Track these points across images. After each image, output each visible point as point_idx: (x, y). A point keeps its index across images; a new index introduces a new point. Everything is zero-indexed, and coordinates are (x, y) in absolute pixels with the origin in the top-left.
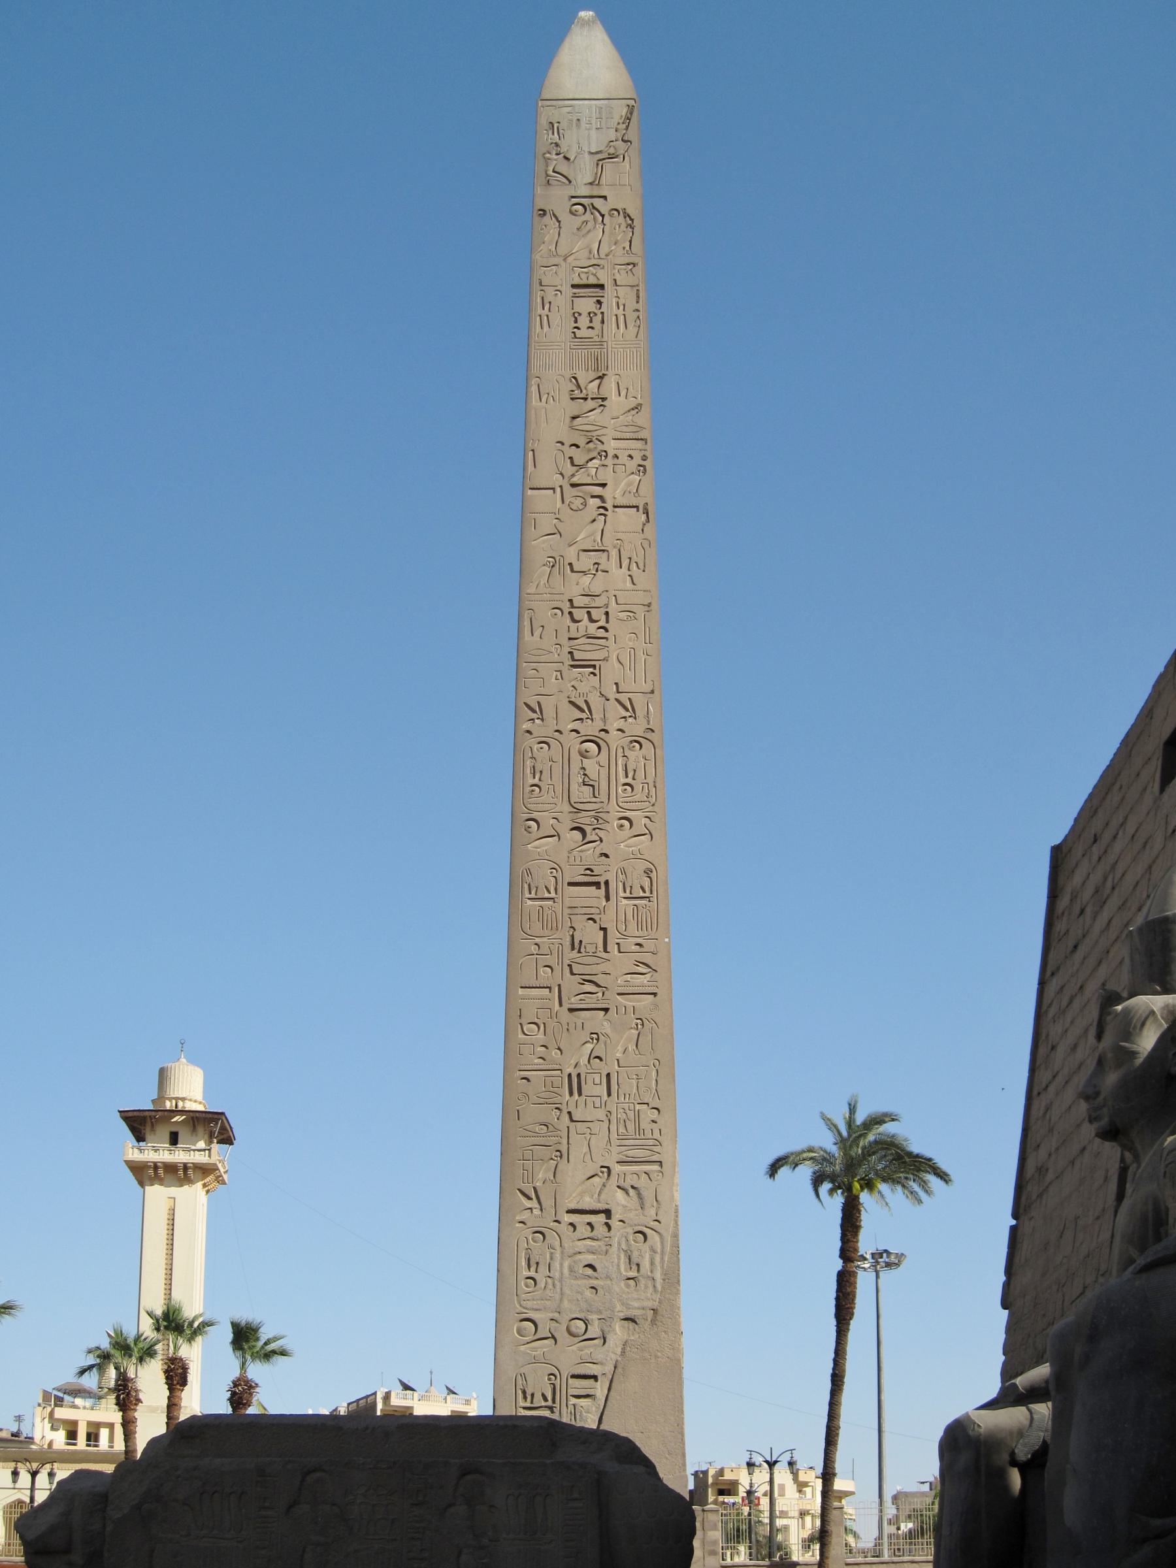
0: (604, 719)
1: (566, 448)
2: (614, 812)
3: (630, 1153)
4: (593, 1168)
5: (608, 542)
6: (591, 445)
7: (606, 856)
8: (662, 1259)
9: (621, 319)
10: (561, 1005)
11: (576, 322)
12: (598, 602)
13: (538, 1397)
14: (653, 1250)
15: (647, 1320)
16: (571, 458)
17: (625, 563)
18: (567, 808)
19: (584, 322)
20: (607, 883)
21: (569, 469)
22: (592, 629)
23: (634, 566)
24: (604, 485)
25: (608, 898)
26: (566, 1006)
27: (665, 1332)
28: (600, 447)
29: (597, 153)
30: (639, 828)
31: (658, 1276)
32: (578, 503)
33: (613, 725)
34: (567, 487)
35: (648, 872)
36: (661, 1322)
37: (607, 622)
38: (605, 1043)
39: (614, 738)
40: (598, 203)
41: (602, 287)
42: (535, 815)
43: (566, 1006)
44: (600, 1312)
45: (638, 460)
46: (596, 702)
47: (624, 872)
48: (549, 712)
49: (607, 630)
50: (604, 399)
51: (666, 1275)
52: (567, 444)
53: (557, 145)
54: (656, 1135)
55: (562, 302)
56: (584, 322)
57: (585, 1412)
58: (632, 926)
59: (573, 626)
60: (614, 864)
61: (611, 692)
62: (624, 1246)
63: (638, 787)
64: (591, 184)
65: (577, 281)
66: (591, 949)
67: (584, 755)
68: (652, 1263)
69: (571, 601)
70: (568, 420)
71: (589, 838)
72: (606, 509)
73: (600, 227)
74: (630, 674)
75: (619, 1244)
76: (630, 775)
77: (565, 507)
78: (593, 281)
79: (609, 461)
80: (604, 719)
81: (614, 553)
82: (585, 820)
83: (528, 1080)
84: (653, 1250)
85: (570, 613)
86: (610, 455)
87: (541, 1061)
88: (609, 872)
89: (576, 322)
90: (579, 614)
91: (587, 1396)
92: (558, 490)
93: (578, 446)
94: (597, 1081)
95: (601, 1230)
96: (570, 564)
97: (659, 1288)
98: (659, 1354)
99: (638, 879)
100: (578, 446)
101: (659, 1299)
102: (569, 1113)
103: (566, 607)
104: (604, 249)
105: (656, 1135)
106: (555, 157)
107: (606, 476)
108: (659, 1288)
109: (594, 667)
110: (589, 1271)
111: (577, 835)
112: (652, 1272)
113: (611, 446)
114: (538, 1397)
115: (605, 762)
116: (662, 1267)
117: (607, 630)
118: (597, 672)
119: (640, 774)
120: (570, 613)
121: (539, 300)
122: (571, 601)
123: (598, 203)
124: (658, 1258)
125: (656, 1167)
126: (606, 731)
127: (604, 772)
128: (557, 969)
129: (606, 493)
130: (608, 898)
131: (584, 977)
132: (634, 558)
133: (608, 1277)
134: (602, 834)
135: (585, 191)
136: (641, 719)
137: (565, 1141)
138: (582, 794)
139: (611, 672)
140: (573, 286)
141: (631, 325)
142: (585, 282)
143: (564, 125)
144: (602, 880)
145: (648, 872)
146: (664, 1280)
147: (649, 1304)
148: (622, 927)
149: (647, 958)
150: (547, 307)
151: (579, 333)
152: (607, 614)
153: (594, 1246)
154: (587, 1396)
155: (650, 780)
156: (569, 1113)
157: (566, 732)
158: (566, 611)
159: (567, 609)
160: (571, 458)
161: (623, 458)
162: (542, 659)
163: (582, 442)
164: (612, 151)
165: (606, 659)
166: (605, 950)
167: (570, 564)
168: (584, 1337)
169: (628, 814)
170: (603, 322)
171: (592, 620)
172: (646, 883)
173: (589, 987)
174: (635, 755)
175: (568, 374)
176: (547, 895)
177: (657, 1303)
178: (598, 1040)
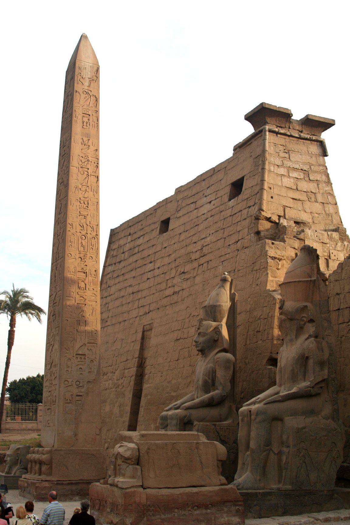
0: (87, 230)
1: (80, 157)
2: (89, 255)
3: (90, 341)
4: (82, 344)
5: (89, 184)
6: (86, 158)
7: (87, 266)
9: (94, 125)
10: (75, 302)
11: (83, 123)
12: (87, 199)
13: (69, 400)
16: (81, 160)
17: (92, 190)
18: (78, 252)
19: (85, 124)
20: (86, 272)
21: (80, 163)
22: (85, 206)
23: (94, 191)
24: (88, 169)
25: (86, 276)
26: (76, 302)
28: (88, 159)
29: (89, 78)
30: (94, 259)
32: (82, 173)
33: (89, 232)
34: (80, 168)
35: (96, 271)
37: (88, 205)
38: (85, 313)
39: (89, 235)
40: (89, 92)
41: (89, 115)
42: (71, 253)
43: (76, 302)
45: (96, 164)
46: (85, 226)
47: (90, 270)
48: (74, 227)
49: (88, 207)
50: (89, 146)
52: (80, 156)
53: (80, 73)
54: (96, 337)
55: (80, 117)
56: (85, 124)
58: (92, 284)
59: (80, 204)
60: (88, 268)
61: (88, 223)
63: (94, 249)
64: (88, 86)
65: (84, 112)
66: (82, 289)
67: (82, 238)
69: (80, 198)
70: (81, 150)
71: (83, 260)
72: (89, 175)
73: (89, 99)
74: (93, 220)
76: (92, 246)
77: (79, 173)
78: (87, 113)
79: (90, 163)
80: (87, 230)
81: (90, 187)
82: (82, 255)
83: (68, 320)
85: (80, 201)
86: (90, 161)
87: (70, 316)
88: (87, 270)
89: (83, 123)
90: (82, 202)
91: (80, 400)
92: (78, 168)
93: (83, 157)
94: (83, 322)
95: (83, 360)
96: (80, 188)
99: (93, 273)
100: (83, 157)
102: (77, 330)
103: (79, 199)
104: (90, 105)
105: (96, 337)
106: (80, 76)
107: (89, 166)
109: (85, 216)
110: (81, 370)
111: (80, 259)
113: (90, 159)
114: (69, 400)
115: (86, 242)
117: (88, 207)
118: (85, 218)
119: (94, 246)
120: (80, 201)
121: (75, 115)
122: (80, 198)
123: (89, 92)
125: (96, 345)
126: (87, 234)
127: (86, 245)
128: (75, 293)
129: (89, 171)
130: (86, 276)
132: (95, 190)
134: (86, 260)
135: (86, 88)
136: (95, 232)
137: (75, 336)
138: (81, 249)
139: (89, 218)
140: (83, 113)
141: (96, 128)
142: (85, 113)
143: (82, 68)
144: (85, 272)
145: (96, 271)
148: (89, 284)
149: (95, 293)
150: (76, 118)
151: (84, 127)
152: (88, 203)
154: (80, 400)
155: (97, 247)
156: (77, 330)
157: (78, 232)
158: (79, 200)
159: (79, 200)
160: (81, 160)
161: (93, 162)
162: (73, 212)
163: (84, 156)
164: (93, 79)
165: (88, 215)
166: (86, 290)
167: (80, 188)
168: (79, 386)
169: (92, 256)
170: (89, 125)
171: (84, 204)
172: (95, 273)
173: (82, 298)
174: (93, 240)
175: (81, 137)
176: (73, 274)
178: (84, 312)
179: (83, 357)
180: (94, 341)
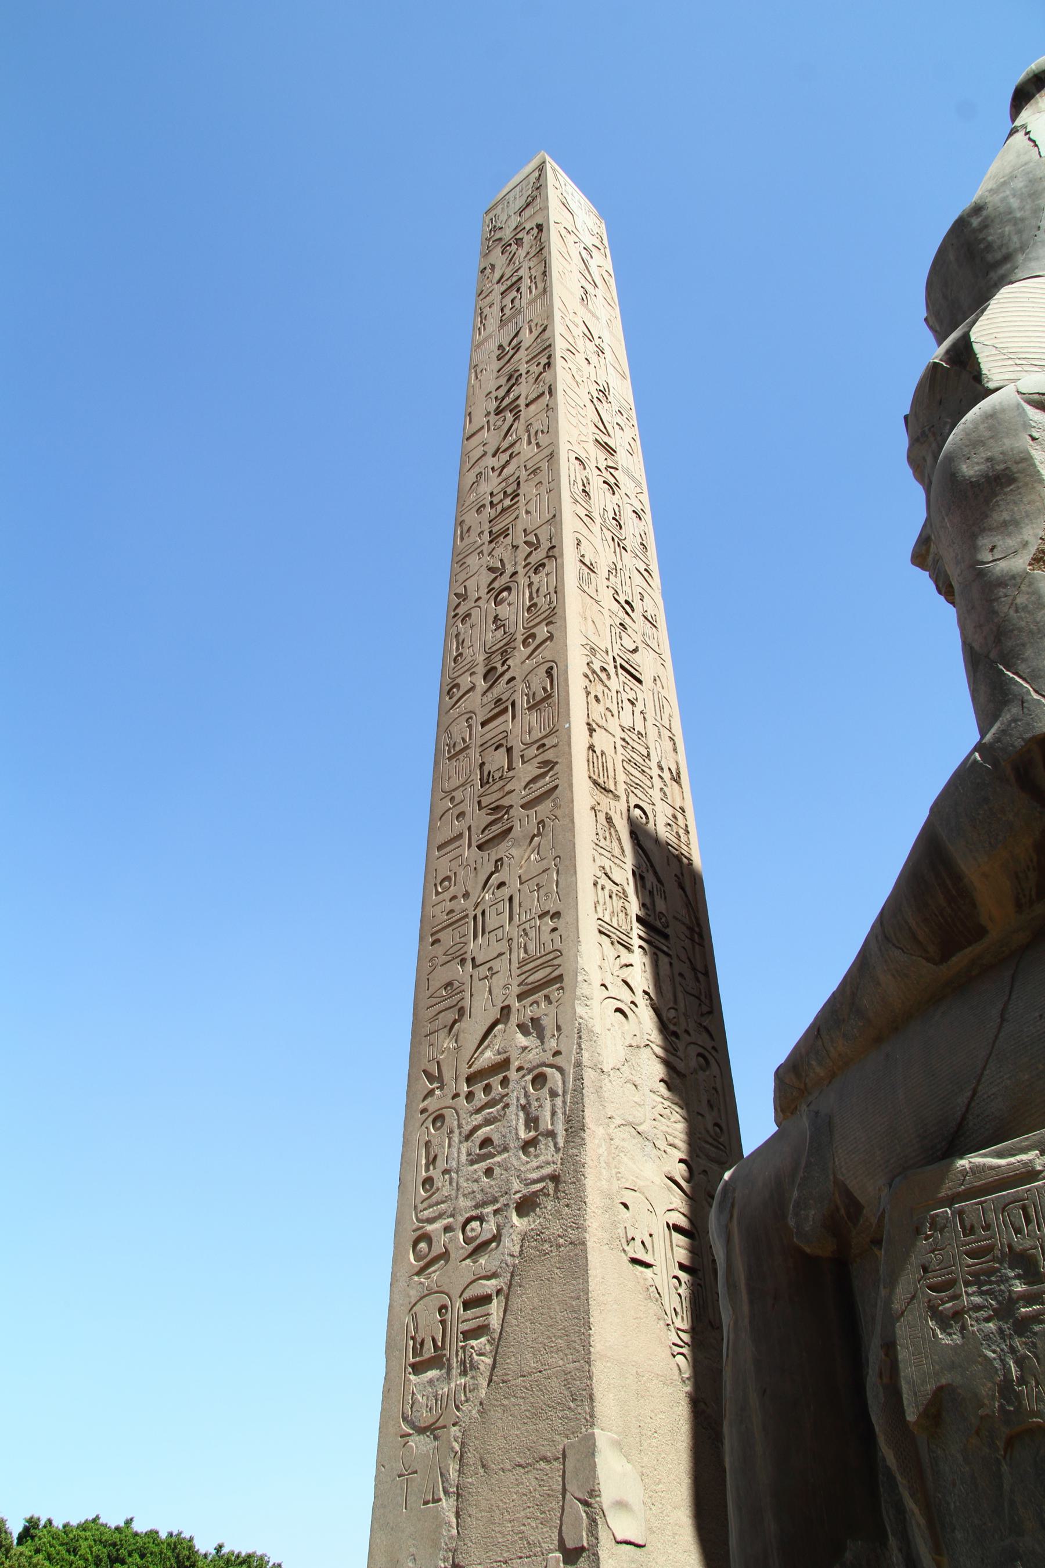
8: (564, 1102)
14: (553, 1094)
15: (549, 1195)
27: (567, 1206)
31: (560, 1129)
36: (564, 1192)
44: (495, 1200)
51: (568, 1120)
54: (558, 944)
57: (477, 1355)
62: (523, 1101)
68: (553, 1113)
75: (518, 1099)
84: (553, 1094)
97: (561, 1144)
98: (561, 1241)
101: (561, 1159)
108: (561, 1144)
112: (552, 1124)
116: (564, 1113)
124: (559, 1101)
131: (489, 807)
133: (506, 1149)
146: (566, 1130)
147: (547, 1171)
153: (492, 1112)
177: (559, 1166)
179: (495, 1081)
180: (548, 970)
